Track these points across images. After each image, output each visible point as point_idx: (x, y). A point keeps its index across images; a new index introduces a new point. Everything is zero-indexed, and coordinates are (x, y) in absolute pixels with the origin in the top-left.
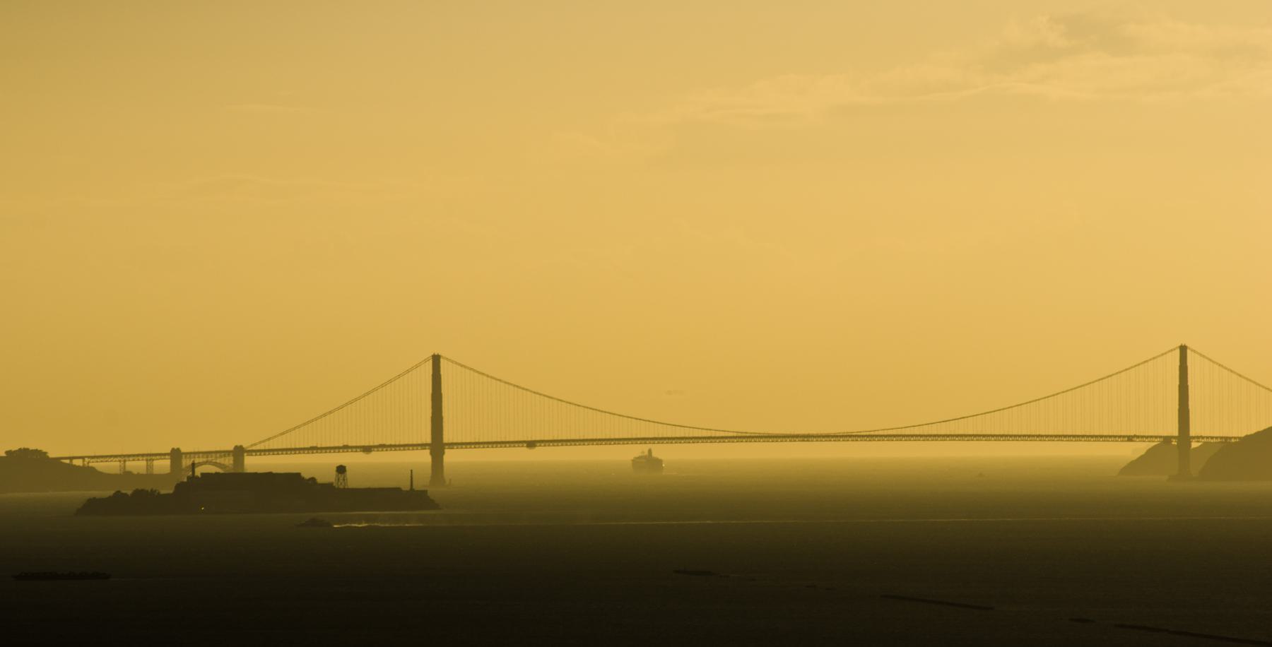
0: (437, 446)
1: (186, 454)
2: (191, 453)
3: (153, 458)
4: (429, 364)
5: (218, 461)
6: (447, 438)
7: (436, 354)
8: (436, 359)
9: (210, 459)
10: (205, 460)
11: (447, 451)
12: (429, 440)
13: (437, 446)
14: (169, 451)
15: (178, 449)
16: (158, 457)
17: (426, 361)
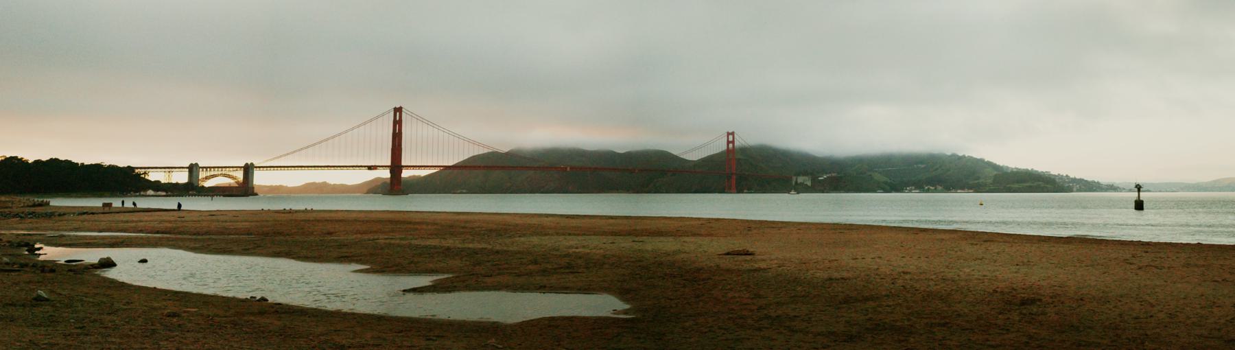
0: (396, 167)
1: (203, 168)
2: (206, 168)
3: (173, 170)
4: (392, 113)
5: (231, 173)
6: (403, 164)
7: (398, 106)
8: (398, 110)
9: (224, 173)
10: (220, 173)
11: (403, 171)
12: (389, 164)
13: (396, 167)
14: (188, 166)
15: (197, 164)
16: (177, 170)
17: (389, 112)
